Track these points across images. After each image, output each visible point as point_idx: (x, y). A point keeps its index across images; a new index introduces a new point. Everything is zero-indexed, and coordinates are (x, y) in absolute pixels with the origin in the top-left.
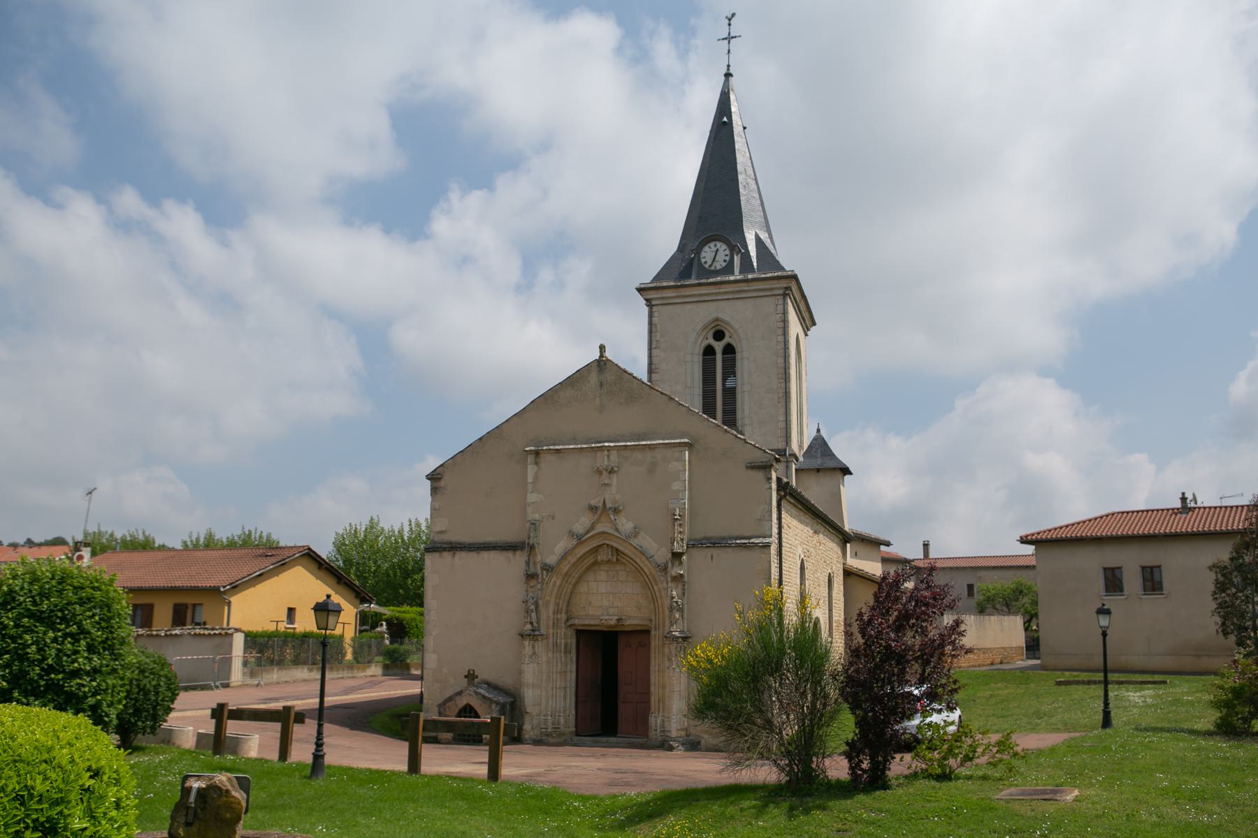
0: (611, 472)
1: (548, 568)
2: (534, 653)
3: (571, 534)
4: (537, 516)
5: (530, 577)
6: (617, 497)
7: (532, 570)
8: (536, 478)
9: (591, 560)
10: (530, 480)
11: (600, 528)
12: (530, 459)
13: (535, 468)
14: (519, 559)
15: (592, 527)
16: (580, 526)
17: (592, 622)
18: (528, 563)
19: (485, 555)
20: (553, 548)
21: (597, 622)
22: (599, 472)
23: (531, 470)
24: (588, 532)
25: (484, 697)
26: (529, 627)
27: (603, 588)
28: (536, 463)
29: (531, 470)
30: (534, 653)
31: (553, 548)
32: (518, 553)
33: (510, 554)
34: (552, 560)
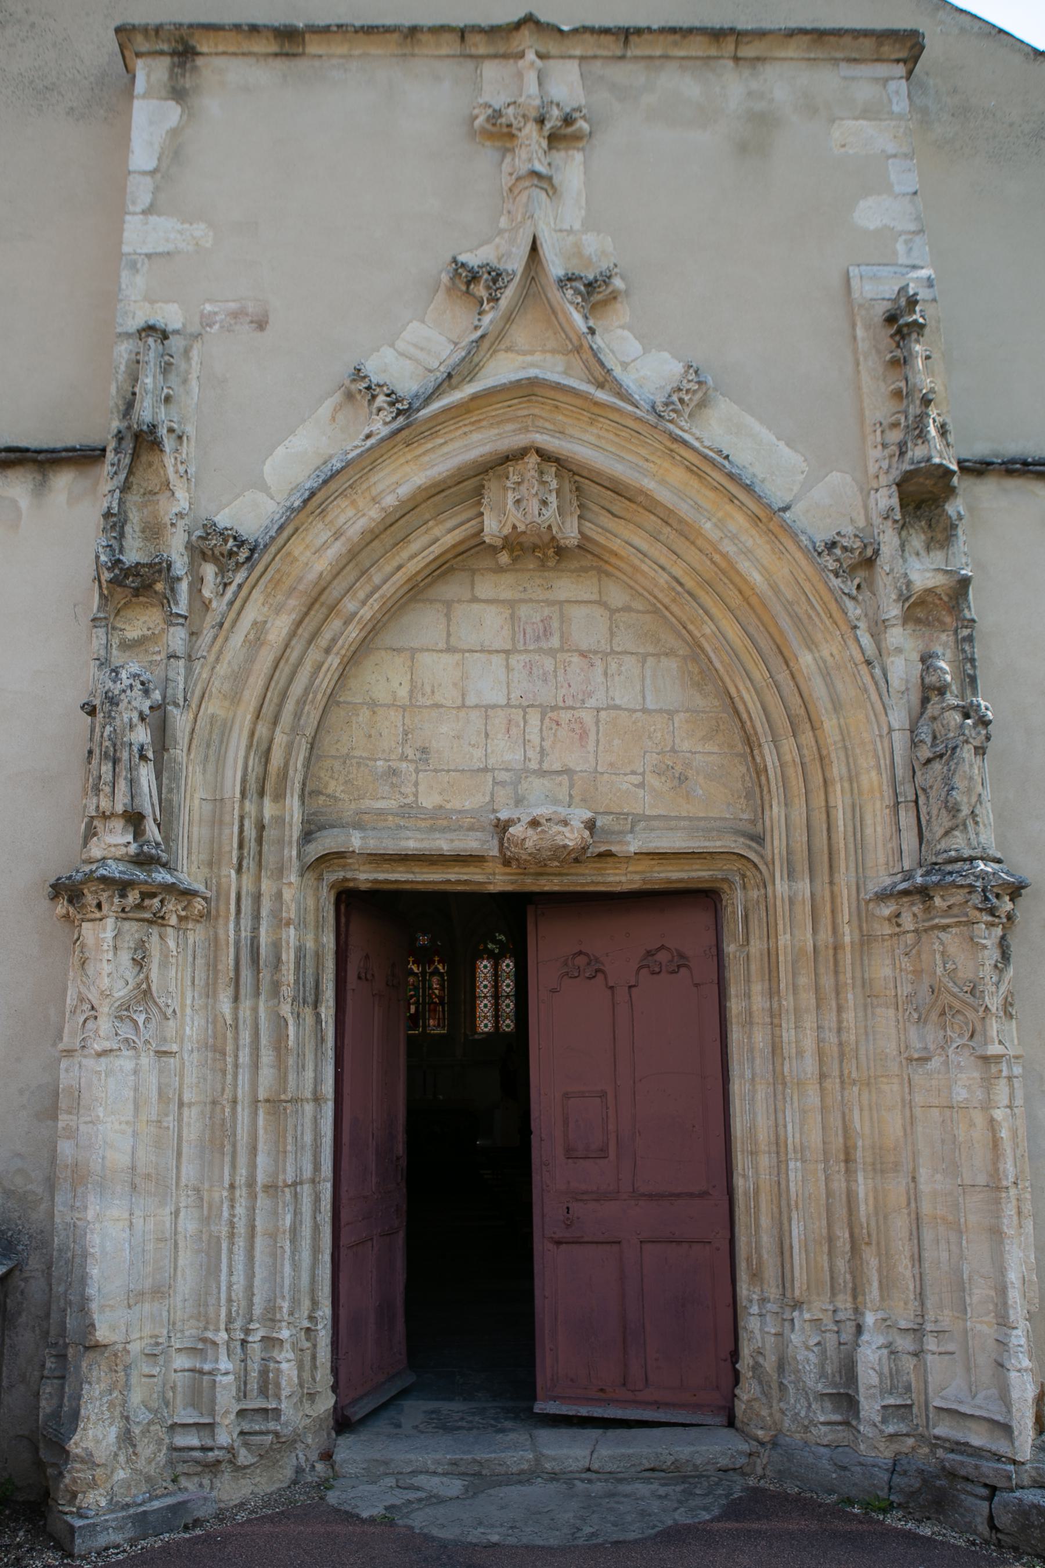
1: (226, 552)
2: (145, 994)
4: (170, 316)
7: (134, 554)
8: (175, 151)
9: (444, 534)
11: (502, 370)
12: (150, 73)
13: (173, 112)
16: (415, 347)
18: (115, 522)
22: (499, 132)
23: (151, 119)
27: (489, 683)
28: (178, 94)
30: (145, 994)
31: (255, 455)
34: (248, 514)
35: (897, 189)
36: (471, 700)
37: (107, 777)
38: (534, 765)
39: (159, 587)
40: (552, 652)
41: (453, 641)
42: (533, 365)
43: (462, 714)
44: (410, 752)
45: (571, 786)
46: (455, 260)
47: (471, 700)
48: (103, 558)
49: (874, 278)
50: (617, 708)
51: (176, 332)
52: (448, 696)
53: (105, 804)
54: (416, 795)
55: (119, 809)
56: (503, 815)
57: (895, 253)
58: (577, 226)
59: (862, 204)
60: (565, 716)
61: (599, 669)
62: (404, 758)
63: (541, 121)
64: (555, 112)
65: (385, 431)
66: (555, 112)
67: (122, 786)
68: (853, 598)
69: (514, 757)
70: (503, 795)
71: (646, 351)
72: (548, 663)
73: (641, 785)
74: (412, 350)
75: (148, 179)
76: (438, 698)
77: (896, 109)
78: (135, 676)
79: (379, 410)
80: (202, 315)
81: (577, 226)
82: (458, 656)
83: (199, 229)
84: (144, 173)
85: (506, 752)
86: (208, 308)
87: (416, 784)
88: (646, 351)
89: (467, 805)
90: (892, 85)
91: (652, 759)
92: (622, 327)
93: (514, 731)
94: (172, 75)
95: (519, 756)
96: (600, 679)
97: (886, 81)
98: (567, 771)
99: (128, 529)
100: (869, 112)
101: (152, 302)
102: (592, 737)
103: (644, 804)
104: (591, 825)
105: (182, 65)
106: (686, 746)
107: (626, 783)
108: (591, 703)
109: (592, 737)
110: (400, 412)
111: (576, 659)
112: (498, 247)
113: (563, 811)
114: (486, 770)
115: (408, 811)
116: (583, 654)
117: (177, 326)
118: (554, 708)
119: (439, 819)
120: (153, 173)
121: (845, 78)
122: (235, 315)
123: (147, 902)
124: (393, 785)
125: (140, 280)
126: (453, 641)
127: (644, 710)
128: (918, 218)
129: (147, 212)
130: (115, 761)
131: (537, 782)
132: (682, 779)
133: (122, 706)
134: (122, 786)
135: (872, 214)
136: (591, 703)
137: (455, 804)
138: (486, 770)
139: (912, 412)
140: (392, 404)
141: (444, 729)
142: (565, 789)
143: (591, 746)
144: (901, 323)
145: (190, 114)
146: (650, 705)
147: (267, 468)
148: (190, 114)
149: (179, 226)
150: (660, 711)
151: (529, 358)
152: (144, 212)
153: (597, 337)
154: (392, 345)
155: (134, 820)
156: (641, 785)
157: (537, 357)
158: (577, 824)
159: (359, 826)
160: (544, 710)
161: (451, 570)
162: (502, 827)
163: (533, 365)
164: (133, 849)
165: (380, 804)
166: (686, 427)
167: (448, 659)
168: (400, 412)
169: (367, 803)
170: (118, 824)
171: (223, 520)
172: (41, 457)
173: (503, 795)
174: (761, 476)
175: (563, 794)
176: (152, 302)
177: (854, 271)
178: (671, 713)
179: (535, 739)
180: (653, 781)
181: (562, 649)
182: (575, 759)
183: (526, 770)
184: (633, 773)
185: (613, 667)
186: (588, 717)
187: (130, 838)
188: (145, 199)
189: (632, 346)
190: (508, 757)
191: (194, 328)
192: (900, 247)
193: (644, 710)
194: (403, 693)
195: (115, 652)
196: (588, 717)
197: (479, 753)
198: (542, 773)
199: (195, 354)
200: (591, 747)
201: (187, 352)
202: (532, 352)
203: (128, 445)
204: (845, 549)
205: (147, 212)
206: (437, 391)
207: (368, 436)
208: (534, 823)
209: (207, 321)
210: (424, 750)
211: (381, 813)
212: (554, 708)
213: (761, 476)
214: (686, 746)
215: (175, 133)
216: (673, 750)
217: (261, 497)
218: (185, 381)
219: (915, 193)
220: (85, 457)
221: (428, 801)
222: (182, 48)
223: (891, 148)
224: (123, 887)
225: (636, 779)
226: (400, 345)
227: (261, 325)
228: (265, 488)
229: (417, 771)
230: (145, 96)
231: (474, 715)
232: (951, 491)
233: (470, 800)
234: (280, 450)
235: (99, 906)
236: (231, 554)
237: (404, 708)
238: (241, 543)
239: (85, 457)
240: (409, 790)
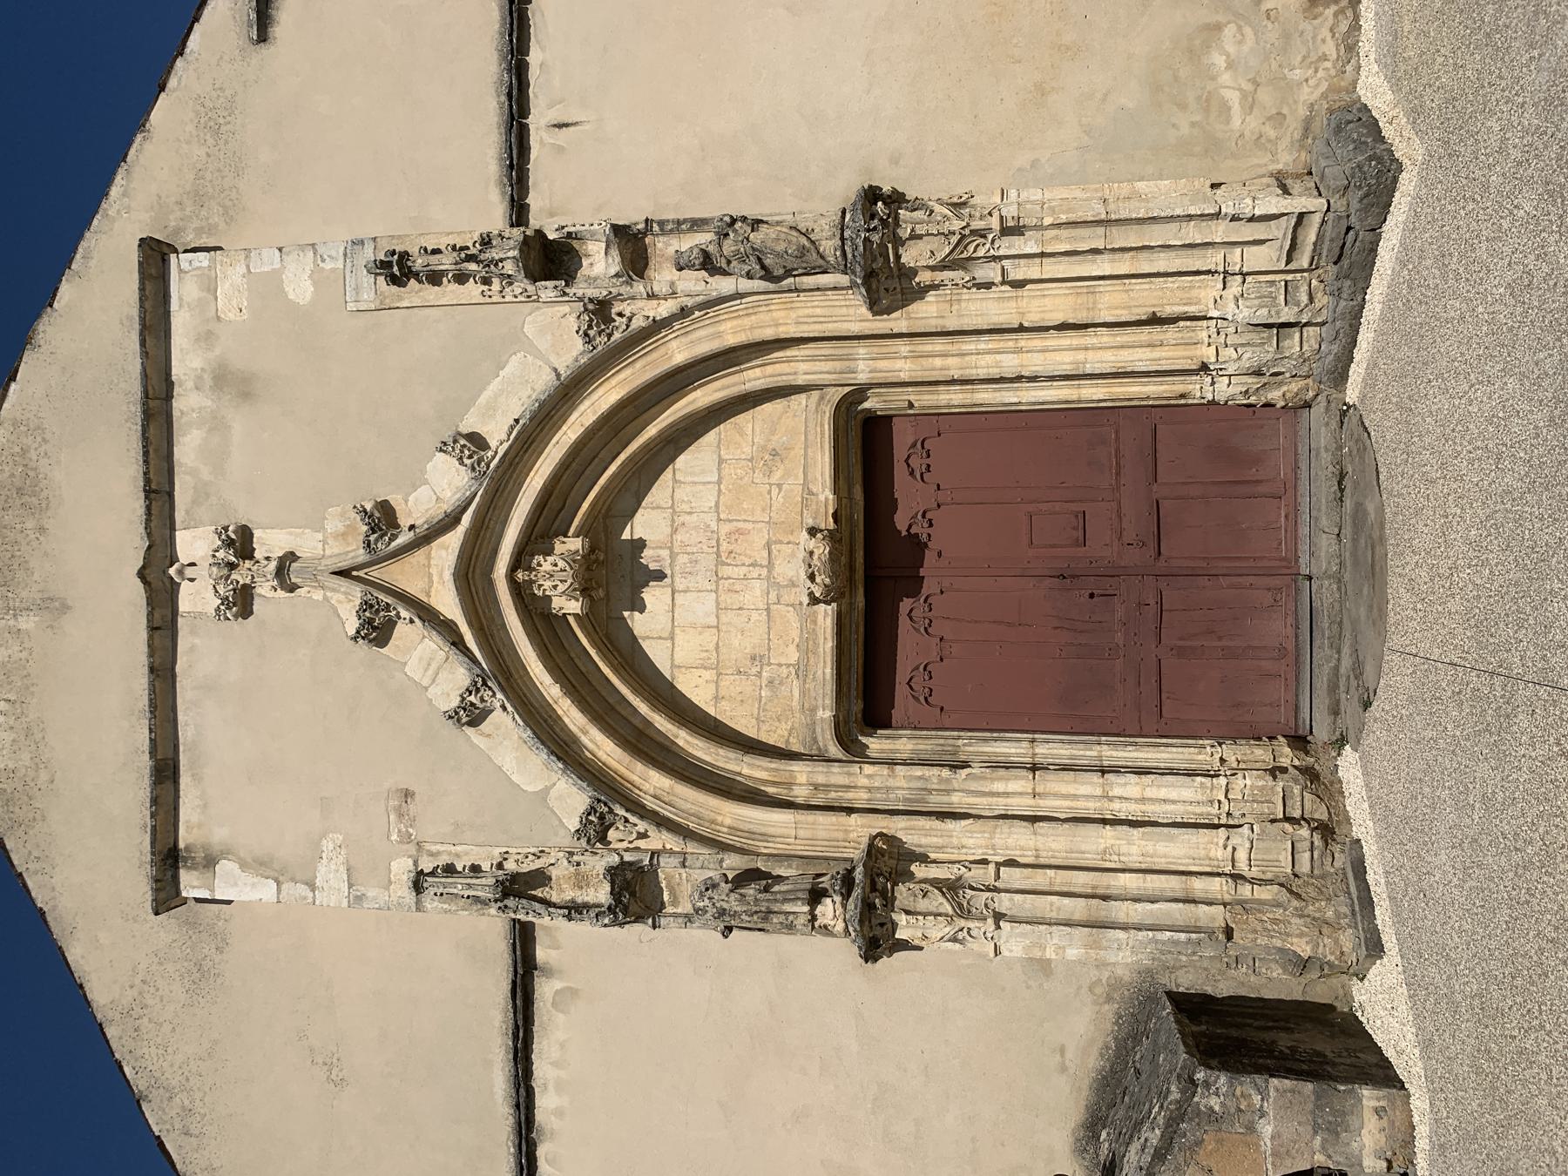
0: (241, 544)
3: (471, 715)
4: (402, 869)
5: (635, 896)
6: (334, 525)
8: (260, 865)
10: (265, 891)
13: (224, 866)
14: (560, 942)
15: (446, 629)
16: (428, 669)
17: (827, 645)
18: (574, 910)
19: (545, 1104)
20: (518, 793)
21: (826, 615)
22: (242, 602)
24: (458, 643)
25: (1160, 1155)
26: (828, 910)
27: (697, 606)
28: (210, 863)
29: (231, 882)
32: (541, 954)
33: (545, 990)
35: (277, 265)
36: (713, 621)
37: (782, 918)
38: (764, 572)
39: (629, 876)
40: (673, 556)
41: (666, 635)
42: (441, 576)
43: (723, 628)
44: (754, 670)
45: (781, 542)
46: (355, 639)
47: (713, 621)
48: (606, 921)
49: (357, 289)
50: (717, 504)
51: (416, 863)
52: (709, 638)
53: (802, 920)
54: (788, 666)
55: (806, 909)
56: (806, 600)
57: (333, 270)
58: (320, 536)
59: (291, 296)
60: (724, 546)
61: (685, 518)
62: (759, 675)
63: (232, 566)
64: (221, 554)
65: (499, 695)
66: (221, 554)
67: (788, 907)
68: (630, 319)
69: (758, 587)
70: (790, 596)
71: (426, 482)
72: (682, 559)
73: (779, 486)
74: (430, 672)
75: (284, 887)
76: (712, 647)
77: (206, 263)
78: (702, 895)
79: (482, 700)
80: (401, 842)
81: (320, 536)
82: (677, 631)
83: (327, 845)
84: (279, 891)
85: (754, 594)
86: (394, 837)
87: (780, 665)
88: (426, 482)
89: (796, 625)
90: (185, 266)
91: (758, 478)
92: (406, 501)
93: (737, 587)
94: (194, 867)
95: (757, 584)
96: (694, 517)
97: (181, 271)
98: (768, 546)
99: (579, 900)
100: (210, 287)
101: (390, 882)
102: (741, 525)
103: (794, 485)
104: (813, 532)
105: (185, 860)
106: (748, 450)
107: (778, 499)
108: (714, 525)
109: (741, 525)
110: (485, 684)
111: (678, 537)
112: (339, 602)
113: (801, 554)
114: (768, 610)
115: (802, 671)
116: (675, 531)
117: (410, 862)
118: (718, 555)
119: (807, 648)
120: (279, 883)
121: (181, 306)
122: (400, 816)
123: (879, 887)
124: (781, 683)
125: (371, 893)
126: (666, 635)
127: (719, 482)
128: (302, 247)
129: (312, 887)
130: (770, 912)
131: (778, 570)
132: (774, 453)
133: (725, 906)
134: (788, 907)
135: (299, 287)
136: (714, 525)
137: (795, 634)
138: (768, 610)
139: (473, 262)
140: (478, 690)
141: (736, 643)
142: (784, 547)
143: (749, 526)
144: (397, 269)
145: (226, 853)
146: (715, 479)
147: (530, 789)
148: (226, 853)
149: (324, 861)
150: (719, 470)
151: (435, 578)
152: (313, 891)
153: (418, 523)
154: (426, 689)
155: (816, 896)
156: (779, 486)
157: (434, 571)
158: (812, 544)
159: (813, 710)
160: (720, 563)
161: (607, 636)
162: (814, 601)
163: (441, 576)
164: (838, 899)
165: (796, 693)
166: (490, 454)
167: (680, 637)
168: (485, 684)
169: (795, 703)
170: (819, 910)
171: (574, 824)
172: (520, 971)
173: (790, 596)
174: (529, 391)
175: (787, 549)
176: (390, 882)
177: (351, 306)
178: (721, 461)
179: (744, 570)
180: (775, 479)
181: (671, 549)
182: (759, 540)
183: (768, 578)
184: (769, 492)
185: (686, 507)
186: (725, 528)
187: (828, 901)
188: (302, 890)
189: (423, 492)
190: (758, 593)
191: (412, 849)
192: (328, 266)
193: (719, 482)
194: (709, 675)
195: (679, 910)
196: (725, 528)
197: (755, 616)
198: (770, 565)
199: (434, 848)
200: (749, 526)
201: (431, 854)
202: (430, 576)
203: (511, 902)
204: (590, 327)
205: (312, 887)
206: (466, 652)
207: (504, 708)
208: (812, 577)
209: (406, 838)
210: (753, 658)
211: (804, 693)
212: (718, 555)
213: (529, 391)
214: (748, 450)
215: (244, 866)
216: (751, 460)
217: (553, 793)
218: (457, 855)
219: (280, 250)
220: (523, 937)
221: (793, 656)
222: (168, 859)
223: (242, 269)
224: (867, 907)
225: (775, 491)
226: (425, 683)
227: (407, 795)
228: (547, 790)
229: (769, 664)
230: (213, 891)
231: (724, 619)
232: (540, 233)
233: (791, 622)
234: (514, 778)
235: (882, 925)
236: (602, 817)
237: (719, 674)
238: (592, 810)
239: (523, 937)
240: (784, 671)
